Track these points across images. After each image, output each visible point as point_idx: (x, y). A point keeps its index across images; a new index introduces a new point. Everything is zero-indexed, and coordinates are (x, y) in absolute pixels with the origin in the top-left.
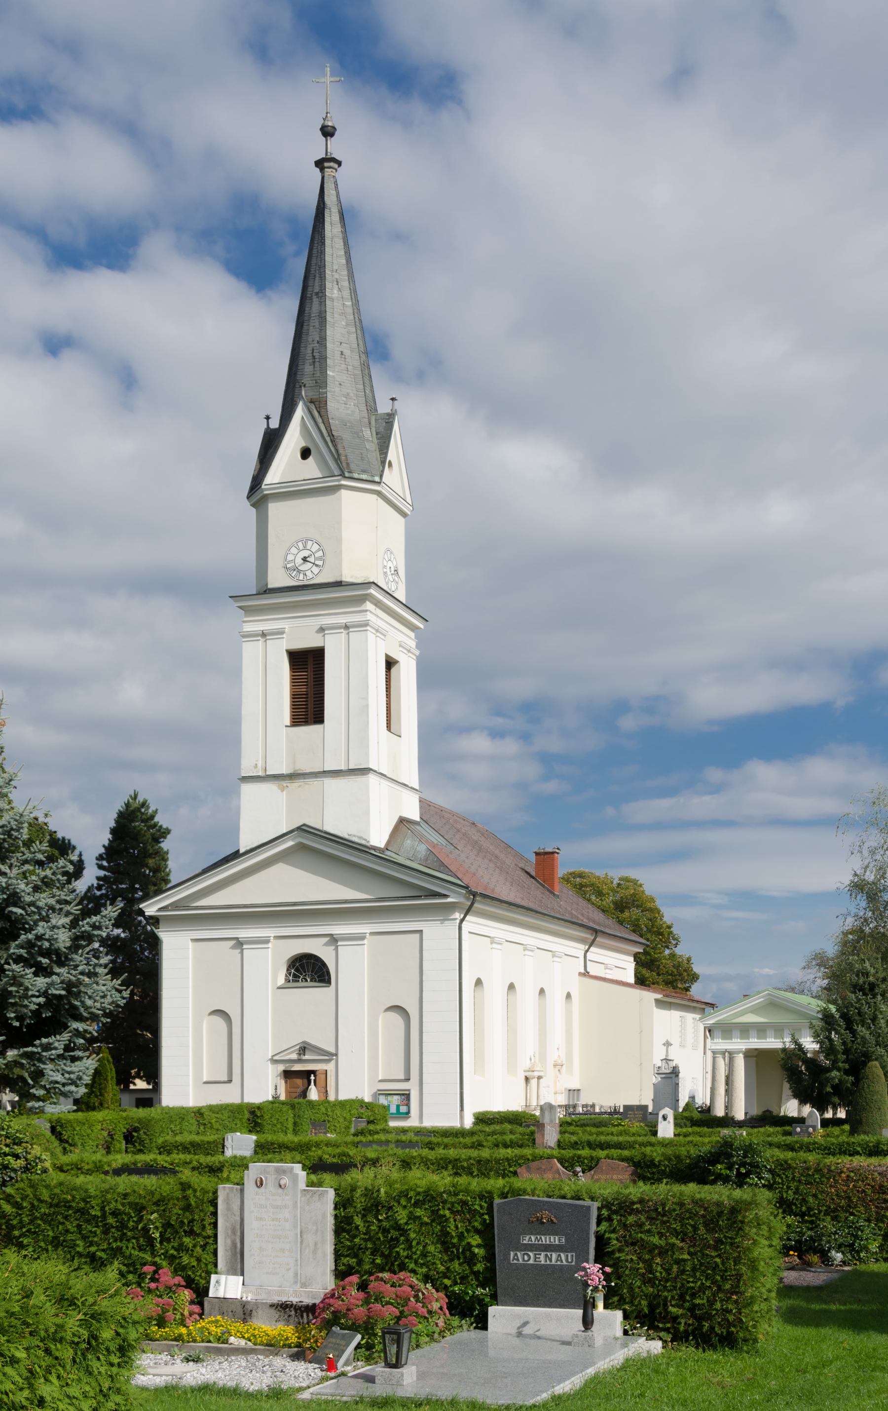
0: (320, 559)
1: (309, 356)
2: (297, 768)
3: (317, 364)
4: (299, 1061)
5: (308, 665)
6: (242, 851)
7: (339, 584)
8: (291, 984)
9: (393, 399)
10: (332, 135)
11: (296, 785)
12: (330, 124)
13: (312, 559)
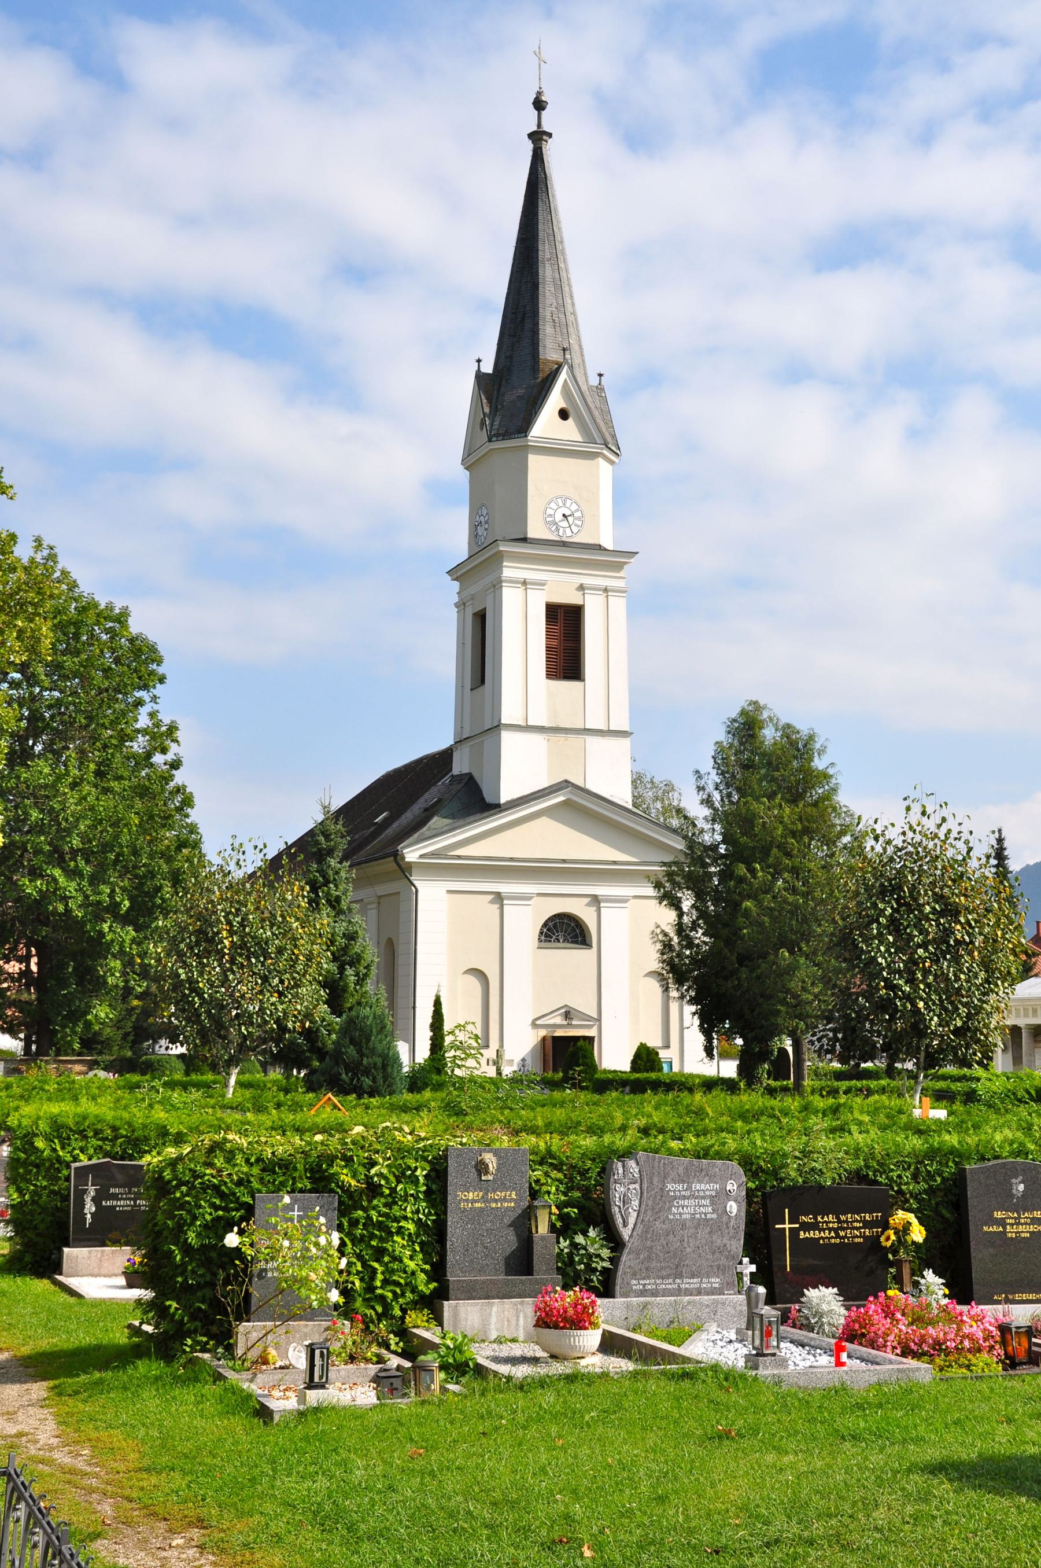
0: (579, 519)
1: (549, 317)
3: (558, 329)
4: (570, 1025)
5: (566, 626)
6: (503, 801)
7: (599, 548)
8: (544, 944)
10: (544, 109)
12: (543, 99)
13: (570, 519)
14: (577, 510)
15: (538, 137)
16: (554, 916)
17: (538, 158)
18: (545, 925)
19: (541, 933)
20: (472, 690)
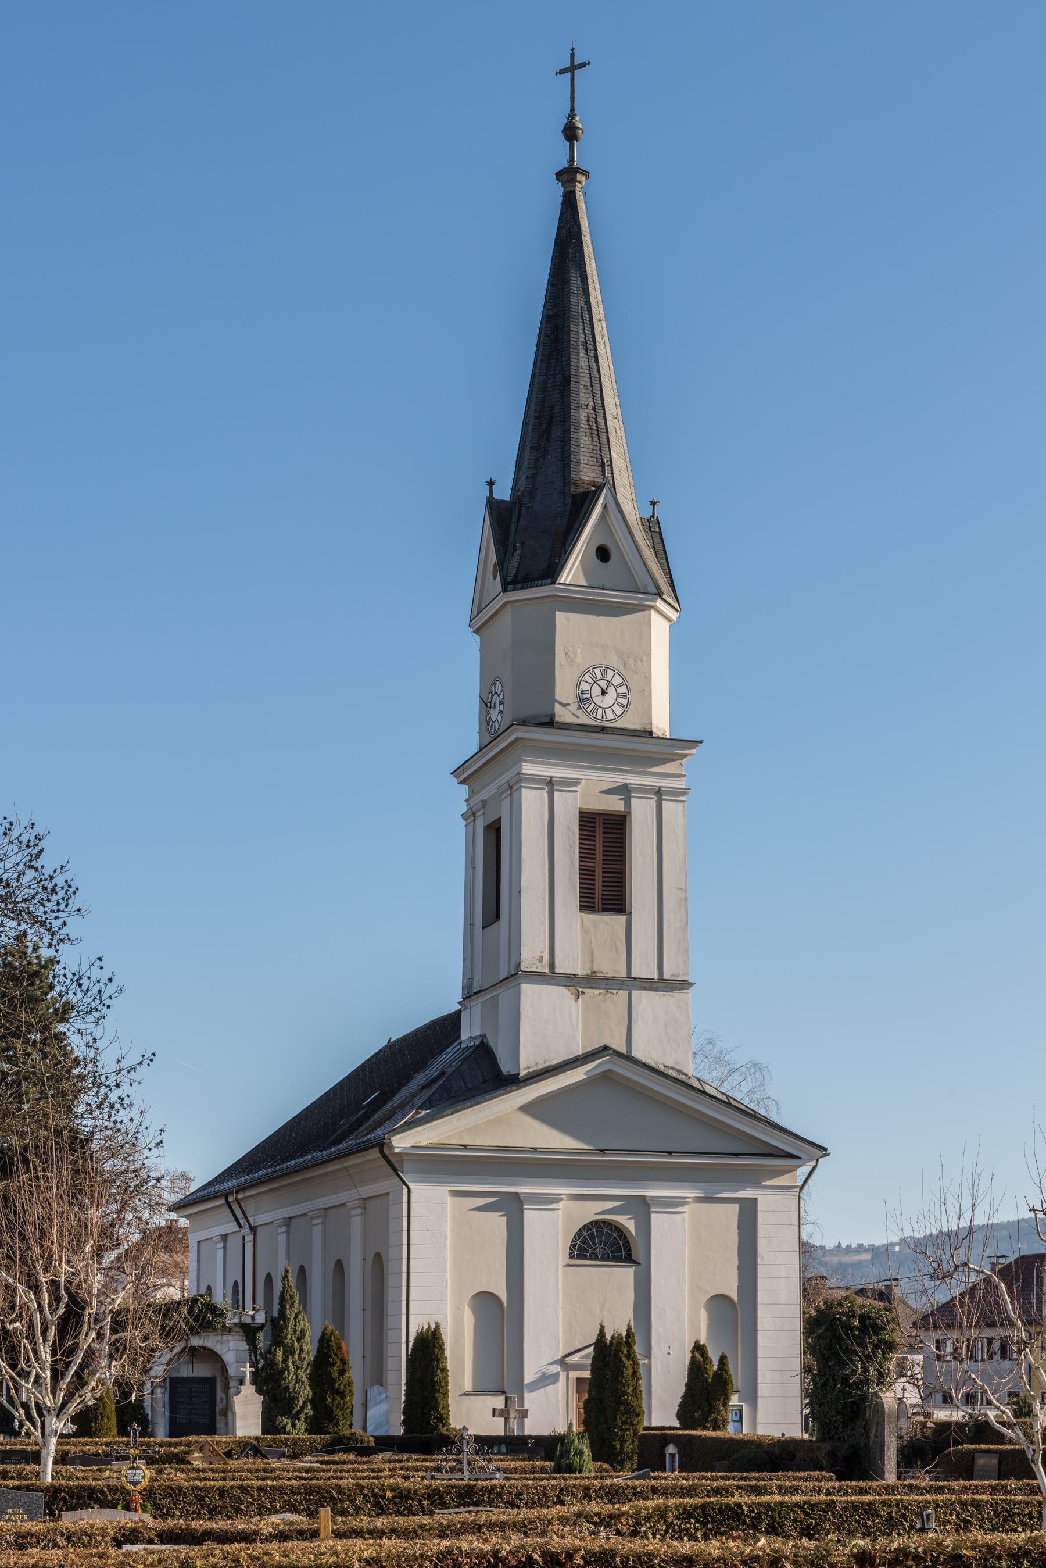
1: (583, 424)
2: (595, 969)
9: (653, 503)
11: (596, 991)
14: (621, 685)
15: (568, 175)
16: (591, 1223)
17: (569, 203)
18: (579, 1234)
19: (573, 1246)
20: (484, 928)
